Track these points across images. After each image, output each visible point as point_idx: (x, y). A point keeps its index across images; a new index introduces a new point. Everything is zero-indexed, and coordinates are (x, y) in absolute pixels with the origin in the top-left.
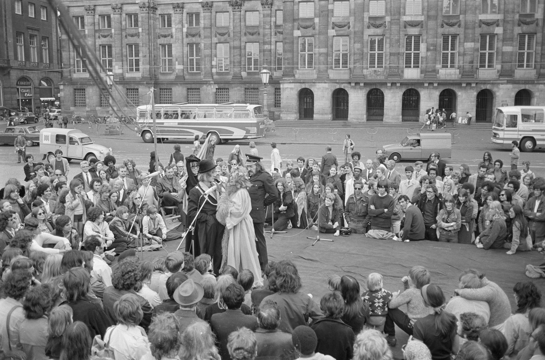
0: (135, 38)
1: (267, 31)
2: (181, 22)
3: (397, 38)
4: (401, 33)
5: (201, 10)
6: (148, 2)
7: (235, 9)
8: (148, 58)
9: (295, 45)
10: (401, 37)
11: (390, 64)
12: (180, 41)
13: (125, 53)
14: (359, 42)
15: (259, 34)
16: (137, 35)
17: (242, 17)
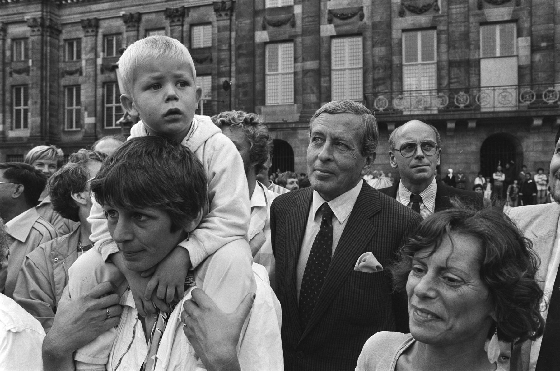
0: (24, 76)
1: (224, 55)
2: (94, 49)
3: (463, 29)
4: (472, 19)
5: (124, 28)
6: (42, 18)
7: (173, 21)
8: (38, 106)
9: (258, 60)
10: (473, 29)
11: (450, 83)
12: (91, 80)
13: (8, 100)
14: (382, 44)
15: (211, 60)
16: (26, 70)
17: (185, 35)
